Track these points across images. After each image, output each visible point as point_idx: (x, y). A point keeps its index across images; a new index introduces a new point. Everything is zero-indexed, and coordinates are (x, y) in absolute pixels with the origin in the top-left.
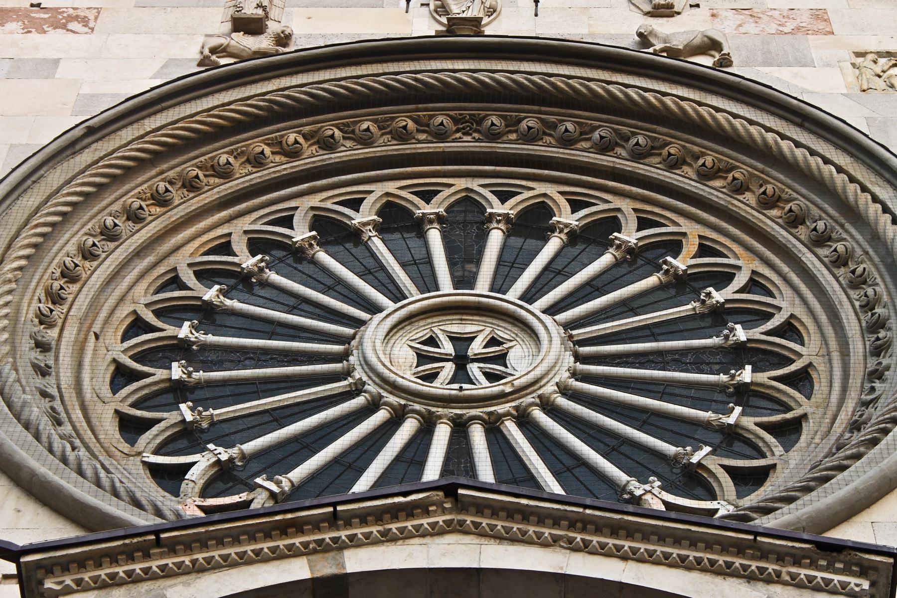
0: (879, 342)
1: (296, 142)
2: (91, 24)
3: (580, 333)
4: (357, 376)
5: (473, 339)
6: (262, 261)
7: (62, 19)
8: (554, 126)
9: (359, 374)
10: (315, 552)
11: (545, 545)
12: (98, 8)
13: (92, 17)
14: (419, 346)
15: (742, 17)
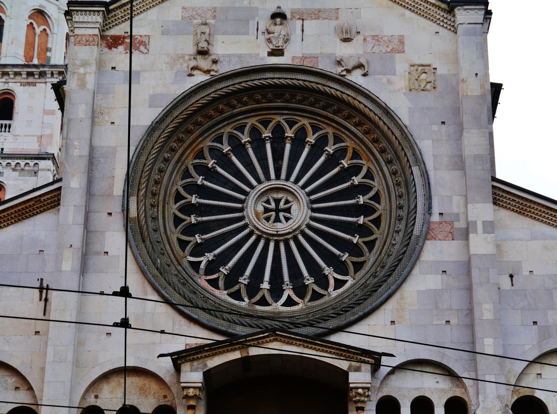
0: (399, 218)
1: (222, 109)
2: (148, 48)
3: (313, 197)
4: (247, 222)
5: (281, 199)
6: (214, 163)
7: (137, 43)
8: (308, 98)
9: (247, 221)
10: (241, 349)
11: (298, 346)
12: (148, 36)
13: (147, 42)
14: (264, 204)
15: (374, 41)
